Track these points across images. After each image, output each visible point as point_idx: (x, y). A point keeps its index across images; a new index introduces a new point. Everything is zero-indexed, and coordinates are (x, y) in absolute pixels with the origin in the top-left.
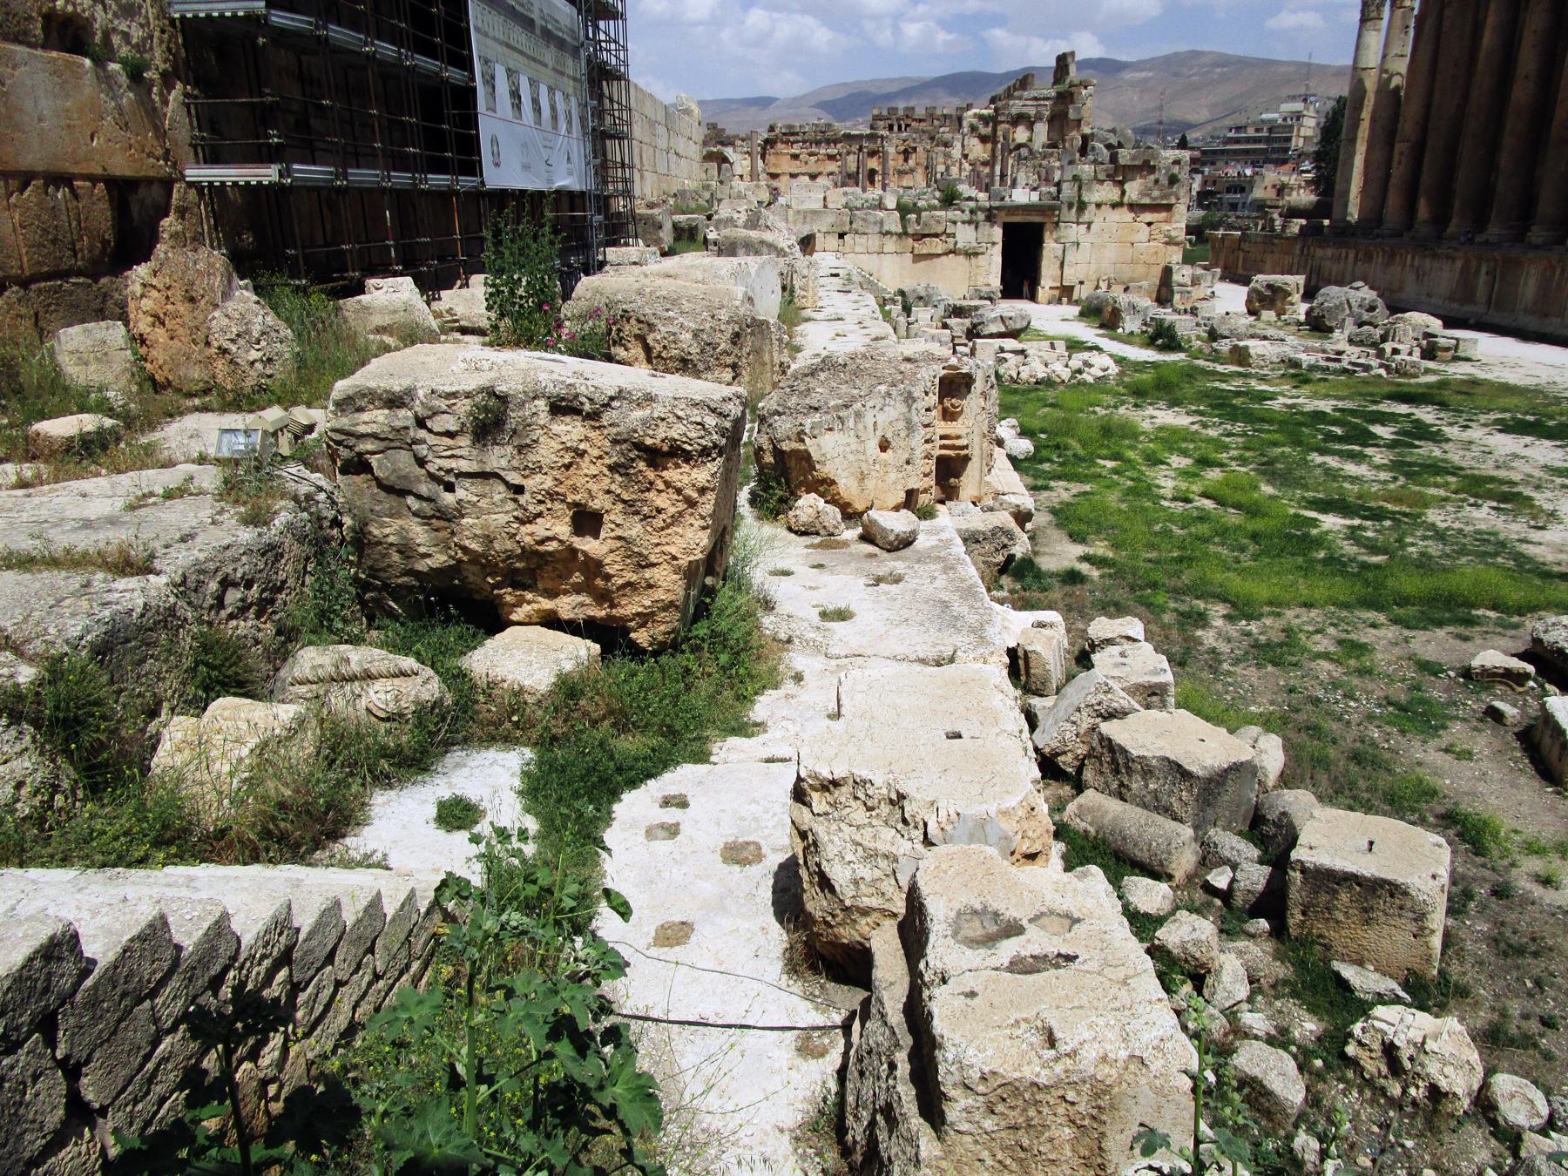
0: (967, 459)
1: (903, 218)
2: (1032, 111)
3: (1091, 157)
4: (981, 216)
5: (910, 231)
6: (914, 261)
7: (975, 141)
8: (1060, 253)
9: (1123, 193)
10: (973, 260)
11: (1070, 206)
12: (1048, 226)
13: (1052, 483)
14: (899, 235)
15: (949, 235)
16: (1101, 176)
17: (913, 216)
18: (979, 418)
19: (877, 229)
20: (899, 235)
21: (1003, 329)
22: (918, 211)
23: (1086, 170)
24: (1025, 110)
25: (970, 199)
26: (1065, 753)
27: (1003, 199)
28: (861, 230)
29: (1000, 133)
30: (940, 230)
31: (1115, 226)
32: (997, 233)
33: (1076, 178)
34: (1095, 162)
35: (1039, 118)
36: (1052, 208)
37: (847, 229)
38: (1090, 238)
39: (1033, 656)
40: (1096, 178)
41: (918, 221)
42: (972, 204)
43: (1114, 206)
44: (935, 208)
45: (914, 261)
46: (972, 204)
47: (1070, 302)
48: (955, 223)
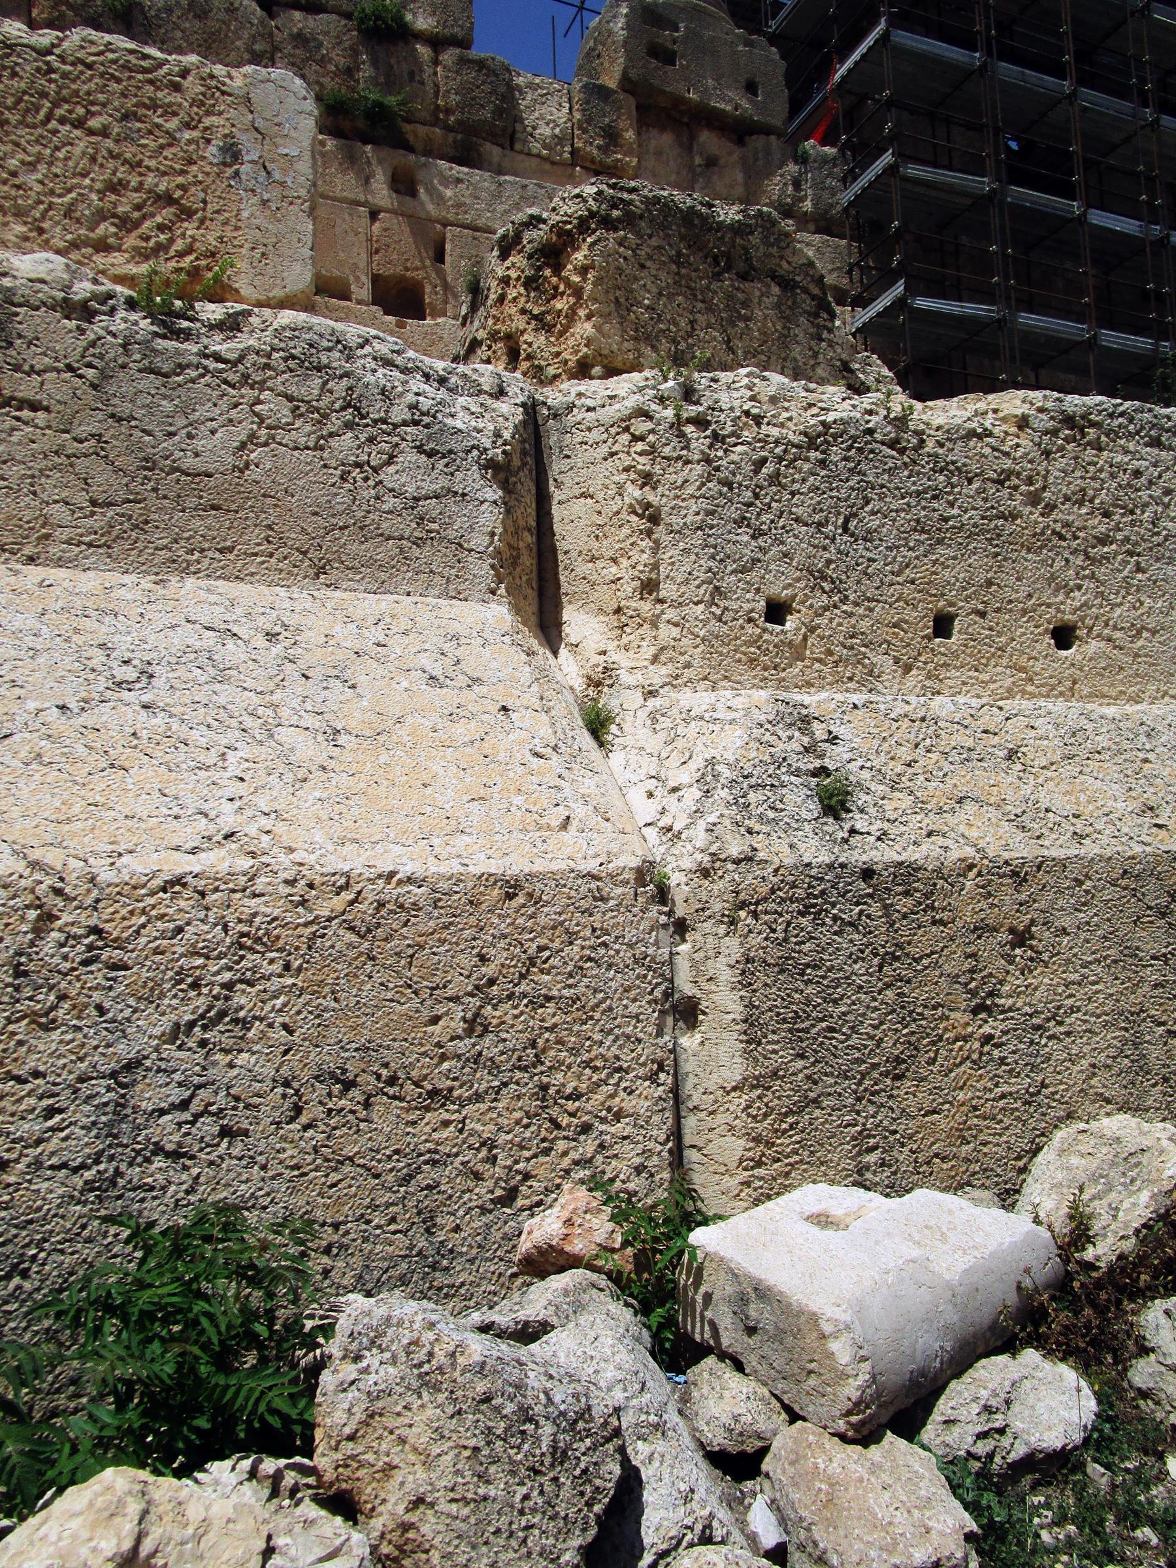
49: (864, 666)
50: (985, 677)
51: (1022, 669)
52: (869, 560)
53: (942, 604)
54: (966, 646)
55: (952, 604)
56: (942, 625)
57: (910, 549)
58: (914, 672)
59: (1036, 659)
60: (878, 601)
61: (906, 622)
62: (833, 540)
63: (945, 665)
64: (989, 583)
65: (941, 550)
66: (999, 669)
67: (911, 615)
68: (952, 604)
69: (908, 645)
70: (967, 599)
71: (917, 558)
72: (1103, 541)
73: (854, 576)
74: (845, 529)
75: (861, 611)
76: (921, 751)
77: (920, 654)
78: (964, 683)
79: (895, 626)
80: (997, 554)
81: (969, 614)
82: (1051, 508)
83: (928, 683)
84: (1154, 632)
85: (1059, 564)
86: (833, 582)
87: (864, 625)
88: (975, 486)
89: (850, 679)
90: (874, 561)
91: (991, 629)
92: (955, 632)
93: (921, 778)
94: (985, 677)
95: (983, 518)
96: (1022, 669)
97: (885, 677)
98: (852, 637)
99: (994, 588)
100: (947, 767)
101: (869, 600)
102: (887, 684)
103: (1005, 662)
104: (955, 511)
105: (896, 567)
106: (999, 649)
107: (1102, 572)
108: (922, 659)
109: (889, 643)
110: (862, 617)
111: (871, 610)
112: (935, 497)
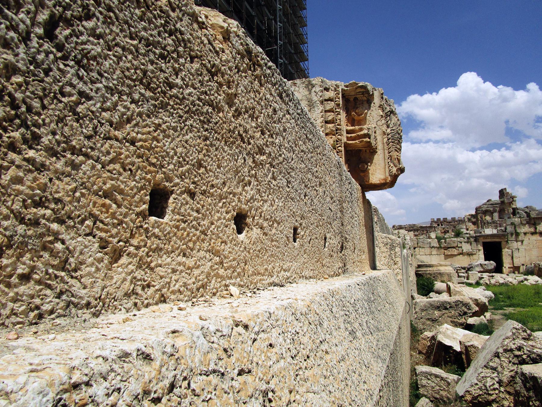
0: (373, 152)
1: (439, 242)
2: (492, 209)
3: (518, 216)
4: (472, 240)
6: (445, 259)
7: (471, 224)
8: (510, 253)
9: (536, 228)
10: (471, 257)
11: (512, 234)
12: (503, 243)
13: (505, 308)
14: (438, 248)
15: (459, 247)
16: (524, 222)
18: (380, 123)
19: (428, 246)
20: (438, 248)
21: (482, 270)
22: (445, 239)
23: (517, 220)
24: (488, 209)
25: (467, 234)
27: (481, 233)
28: (422, 246)
29: (479, 217)
30: (455, 245)
31: (535, 242)
32: (481, 248)
33: (512, 224)
34: (520, 217)
35: (495, 211)
36: (503, 235)
37: (416, 246)
38: (523, 247)
40: (521, 223)
41: (445, 242)
42: (468, 235)
43: (532, 234)
44: (453, 238)
45: (445, 259)
46: (468, 235)
47: (519, 273)
49: (54, 254)
50: (190, 262)
51: (217, 253)
52: (81, 94)
53: (160, 176)
54: (177, 227)
55: (169, 179)
56: (158, 202)
57: (133, 101)
58: (124, 260)
59: (225, 242)
60: (87, 156)
61: (121, 192)
62: (26, 38)
63: (158, 250)
64: (200, 165)
65: (163, 115)
66: (202, 253)
67: (127, 183)
68: (169, 179)
69: (121, 223)
70: (182, 177)
71: (140, 114)
72: (261, 152)
73: (54, 109)
74: (50, 34)
75: (60, 165)
77: (132, 236)
78: (174, 271)
79: (106, 195)
80: (206, 139)
81: (182, 193)
82: (238, 114)
83: (139, 274)
84: (279, 224)
85: (240, 161)
86: (14, 105)
87: (62, 188)
88: (196, 65)
89: (25, 278)
90: (89, 98)
91: (198, 211)
92: (169, 210)
94: (190, 262)
95: (199, 99)
96: (217, 253)
97: (85, 269)
98: (39, 204)
99: (202, 170)
101: (74, 151)
102: (87, 281)
103: (205, 245)
104: (179, 81)
105: (116, 118)
106: (203, 232)
107: (260, 174)
108: (135, 242)
109: (96, 219)
110: (60, 175)
111: (75, 167)
112: (162, 57)
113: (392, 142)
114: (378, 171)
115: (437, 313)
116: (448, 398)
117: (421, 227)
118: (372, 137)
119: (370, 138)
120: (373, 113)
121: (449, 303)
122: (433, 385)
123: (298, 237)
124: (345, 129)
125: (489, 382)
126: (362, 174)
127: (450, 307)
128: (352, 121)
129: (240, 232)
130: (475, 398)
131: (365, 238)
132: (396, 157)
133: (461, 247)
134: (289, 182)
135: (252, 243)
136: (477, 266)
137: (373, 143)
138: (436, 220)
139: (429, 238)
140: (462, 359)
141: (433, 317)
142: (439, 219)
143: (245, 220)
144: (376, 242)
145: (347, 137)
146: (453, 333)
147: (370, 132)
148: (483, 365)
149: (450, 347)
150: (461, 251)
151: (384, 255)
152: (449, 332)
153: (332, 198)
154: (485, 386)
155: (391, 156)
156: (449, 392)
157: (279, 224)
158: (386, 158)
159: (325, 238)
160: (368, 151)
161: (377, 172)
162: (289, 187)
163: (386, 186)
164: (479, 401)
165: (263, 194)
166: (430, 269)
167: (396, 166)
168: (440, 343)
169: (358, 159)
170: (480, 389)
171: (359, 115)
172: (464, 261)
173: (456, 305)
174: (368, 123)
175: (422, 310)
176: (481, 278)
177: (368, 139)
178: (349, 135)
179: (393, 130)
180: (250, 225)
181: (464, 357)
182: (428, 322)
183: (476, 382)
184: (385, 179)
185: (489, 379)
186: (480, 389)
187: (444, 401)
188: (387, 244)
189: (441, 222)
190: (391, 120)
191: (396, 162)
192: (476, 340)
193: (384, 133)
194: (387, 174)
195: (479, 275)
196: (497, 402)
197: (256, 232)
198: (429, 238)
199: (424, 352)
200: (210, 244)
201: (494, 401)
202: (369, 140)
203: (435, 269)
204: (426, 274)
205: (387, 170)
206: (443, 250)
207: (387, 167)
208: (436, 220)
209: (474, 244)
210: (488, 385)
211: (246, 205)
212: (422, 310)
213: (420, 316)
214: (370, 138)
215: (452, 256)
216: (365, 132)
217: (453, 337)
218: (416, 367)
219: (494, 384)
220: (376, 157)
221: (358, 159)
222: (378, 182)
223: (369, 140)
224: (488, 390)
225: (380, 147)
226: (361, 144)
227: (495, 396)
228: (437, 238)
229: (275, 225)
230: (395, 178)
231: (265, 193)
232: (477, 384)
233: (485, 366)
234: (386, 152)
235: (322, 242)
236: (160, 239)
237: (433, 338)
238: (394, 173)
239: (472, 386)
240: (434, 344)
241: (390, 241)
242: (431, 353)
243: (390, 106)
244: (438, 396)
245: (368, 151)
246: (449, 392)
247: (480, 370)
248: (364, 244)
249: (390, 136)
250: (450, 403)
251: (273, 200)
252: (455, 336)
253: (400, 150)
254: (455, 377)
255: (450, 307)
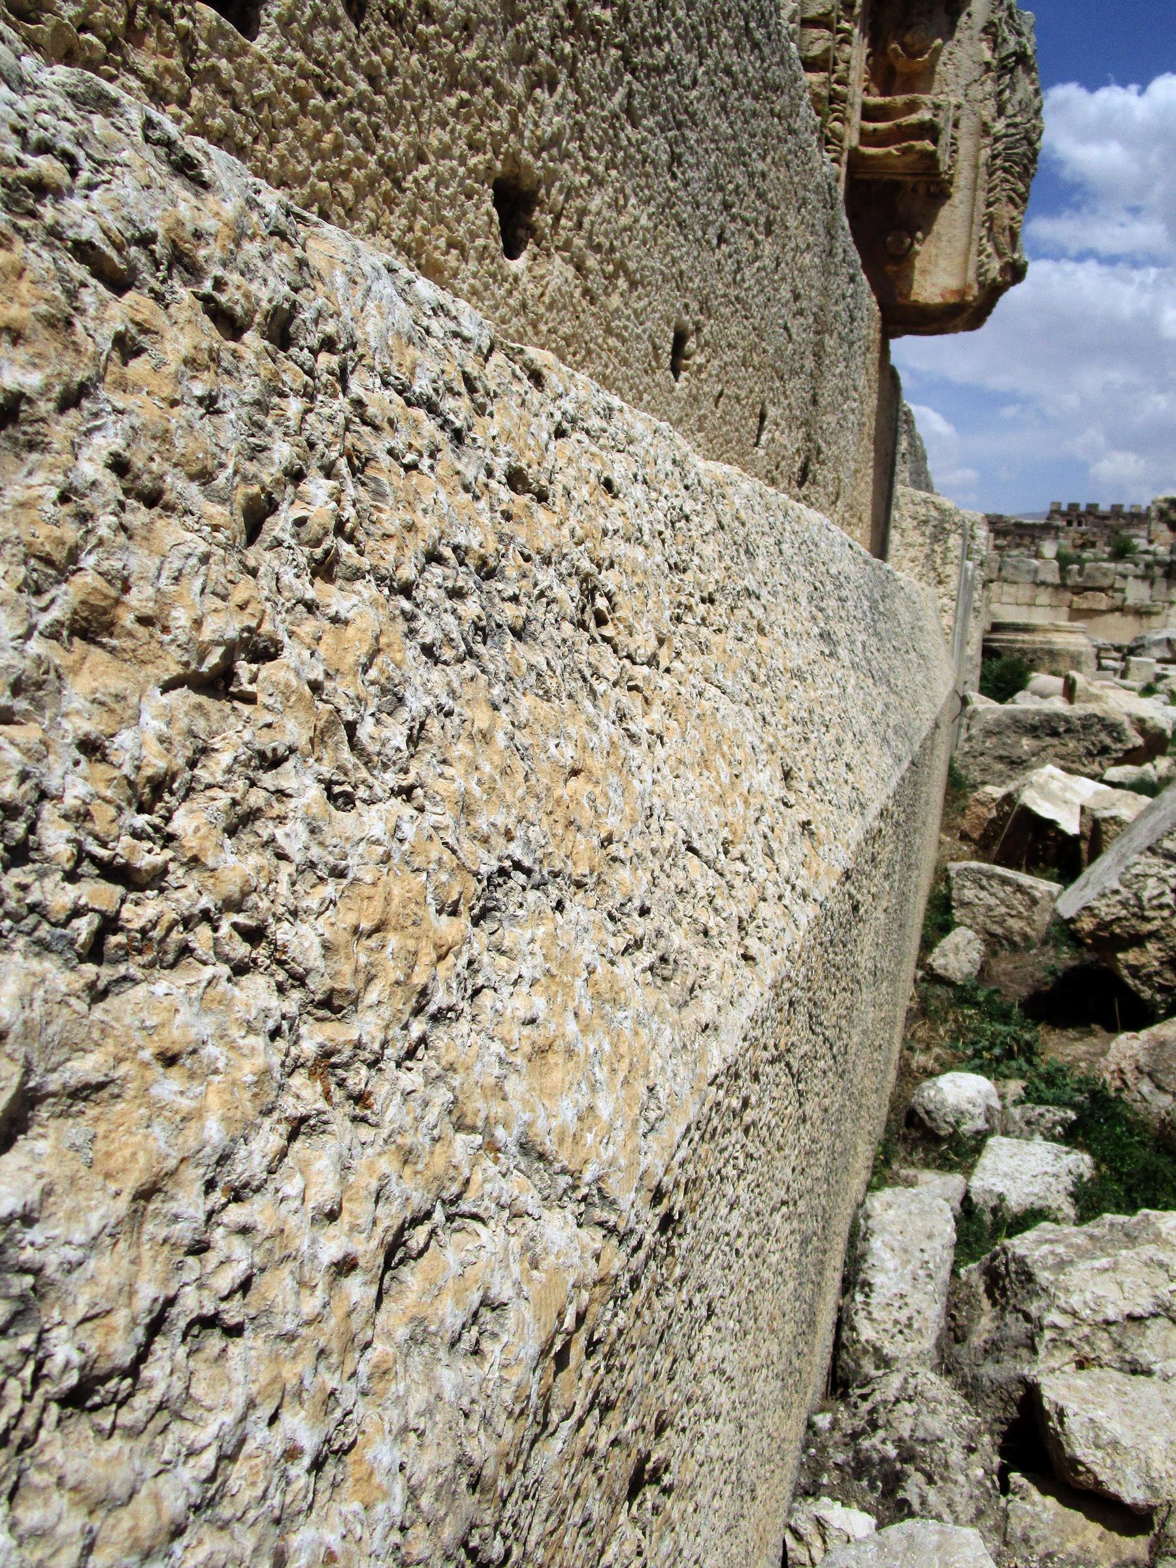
0: (937, 191)
1: (1063, 570)
4: (1158, 571)
5: (1069, 582)
7: (1163, 527)
10: (1145, 621)
14: (1056, 587)
17: (1075, 567)
18: (976, 92)
19: (1029, 578)
20: (1056, 587)
21: (1168, 655)
22: (1080, 561)
25: (1147, 552)
26: (1137, 940)
30: (1106, 582)
39: (1112, 828)
42: (1149, 558)
46: (1149, 558)
48: (1125, 577)
76: (281, 566)
93: (302, 784)
100: (425, 687)
106: (389, 169)
113: (1005, 170)
114: (943, 263)
115: (1027, 743)
116: (1026, 937)
117: (1019, 525)
118: (944, 139)
119: (935, 142)
120: (960, 54)
121: (1067, 720)
122: (993, 901)
123: (686, 368)
124: (858, 101)
125: (1151, 888)
126: (891, 268)
127: (1067, 731)
128: (885, 76)
129: (512, 252)
130: (1104, 925)
131: (869, 479)
132: (1007, 222)
133: (1122, 590)
134: (675, 158)
135: (547, 299)
136: (1157, 643)
137: (945, 160)
138: (1064, 508)
139: (1038, 555)
140: (1079, 850)
141: (1015, 753)
142: (1073, 507)
143: (530, 212)
144: (895, 514)
145: (863, 133)
146: (1065, 788)
147: (940, 121)
148: (1147, 844)
149: (1052, 824)
150: (1118, 603)
151: (912, 553)
152: (1055, 786)
153: (797, 297)
154: (1138, 898)
155: (991, 217)
156: (1030, 921)
157: (633, 285)
158: (978, 219)
159: (762, 417)
160: (922, 191)
161: (939, 269)
162: (674, 177)
163: (958, 321)
164: (1113, 934)
165: (594, 153)
166: (1026, 637)
167: (1000, 254)
168: (1027, 813)
169: (888, 207)
170: (1124, 904)
171: (913, 56)
172: (1122, 630)
173: (1084, 727)
174: (936, 88)
175: (989, 733)
176: (1160, 678)
177: (927, 145)
178: (871, 126)
179: (1015, 125)
180: (543, 237)
181: (1084, 846)
182: (999, 767)
183: (1116, 885)
184: (962, 293)
185: (1151, 882)
186: (1124, 904)
187: (1013, 944)
188: (925, 522)
189: (1079, 516)
190: (1012, 87)
191: (1004, 239)
192: (1128, 806)
193: (985, 129)
194: (971, 274)
195: (1158, 668)
196: (1160, 939)
197: (558, 270)
198: (1038, 555)
199: (976, 835)
200: (411, 229)
201: (1154, 935)
202: (931, 147)
203: (1038, 638)
204: (1012, 650)
205: (973, 259)
206: (1068, 596)
207: (974, 249)
208: (1064, 508)
209: (1161, 584)
210: (1146, 895)
211: (537, 156)
212: (989, 733)
213: (978, 747)
214: (935, 142)
215: (1090, 613)
216: (925, 115)
217: (1060, 796)
218: (950, 865)
219: (1162, 894)
220: (945, 212)
221: (888, 207)
222: (938, 300)
223: (931, 147)
224: (1141, 908)
225: (962, 179)
226: (910, 158)
227: (1157, 923)
228: (1059, 557)
229: (622, 283)
230: (992, 293)
231: (600, 149)
232: (1116, 892)
233: (1150, 849)
234: (982, 195)
235: (753, 422)
236: (236, 108)
237: (1009, 799)
238: (991, 275)
239: (1103, 896)
240: (1007, 814)
241: (934, 513)
242: (995, 838)
243: (1020, 34)
244: (999, 931)
245: (922, 191)
246: (1030, 921)
247: (1135, 858)
248: (864, 494)
249: (1000, 146)
250: (1028, 948)
251: (622, 190)
252: (1068, 795)
253: (1025, 200)
254: (1055, 887)
255: (1067, 731)
